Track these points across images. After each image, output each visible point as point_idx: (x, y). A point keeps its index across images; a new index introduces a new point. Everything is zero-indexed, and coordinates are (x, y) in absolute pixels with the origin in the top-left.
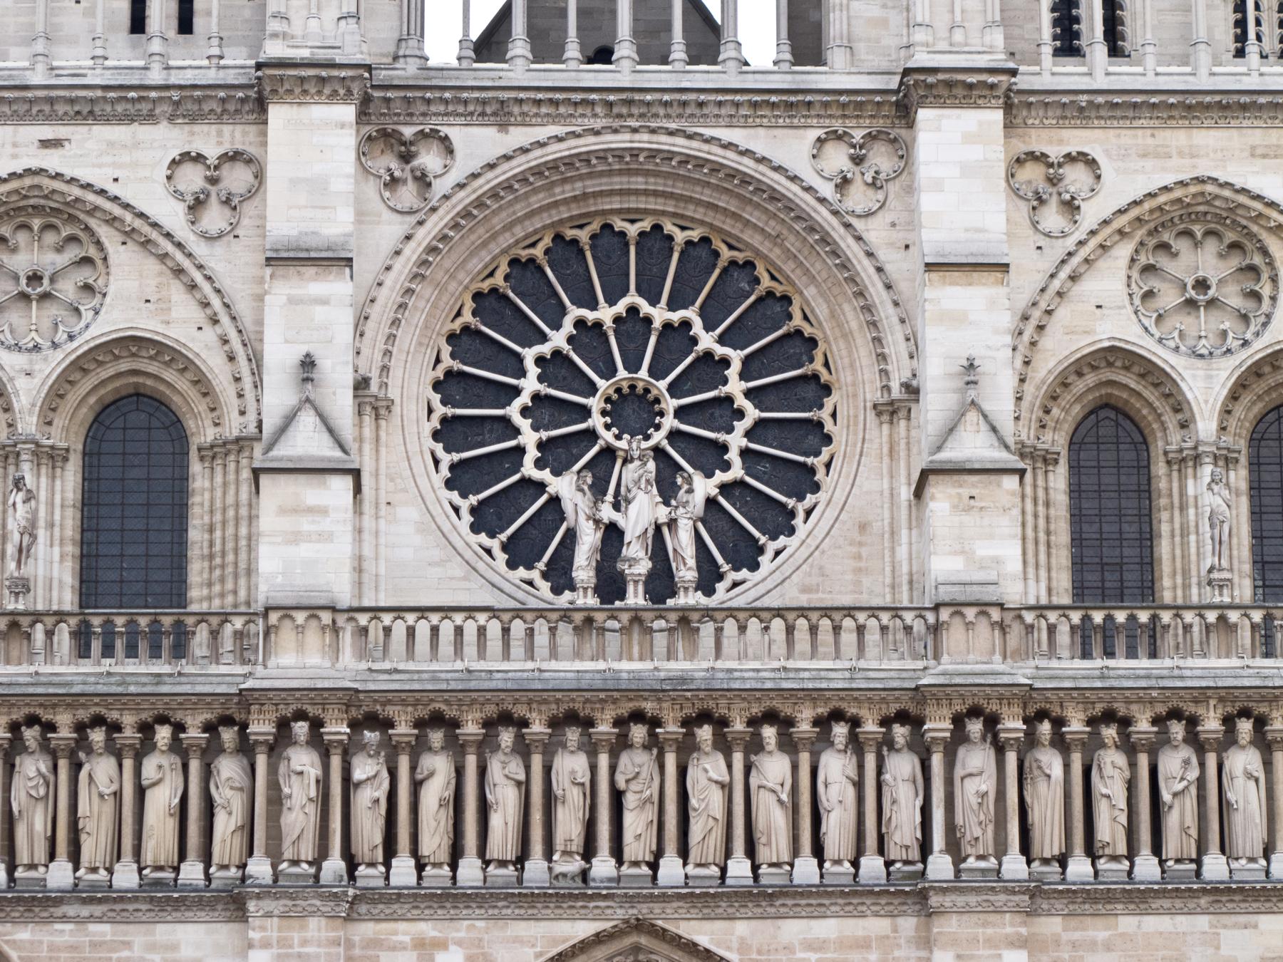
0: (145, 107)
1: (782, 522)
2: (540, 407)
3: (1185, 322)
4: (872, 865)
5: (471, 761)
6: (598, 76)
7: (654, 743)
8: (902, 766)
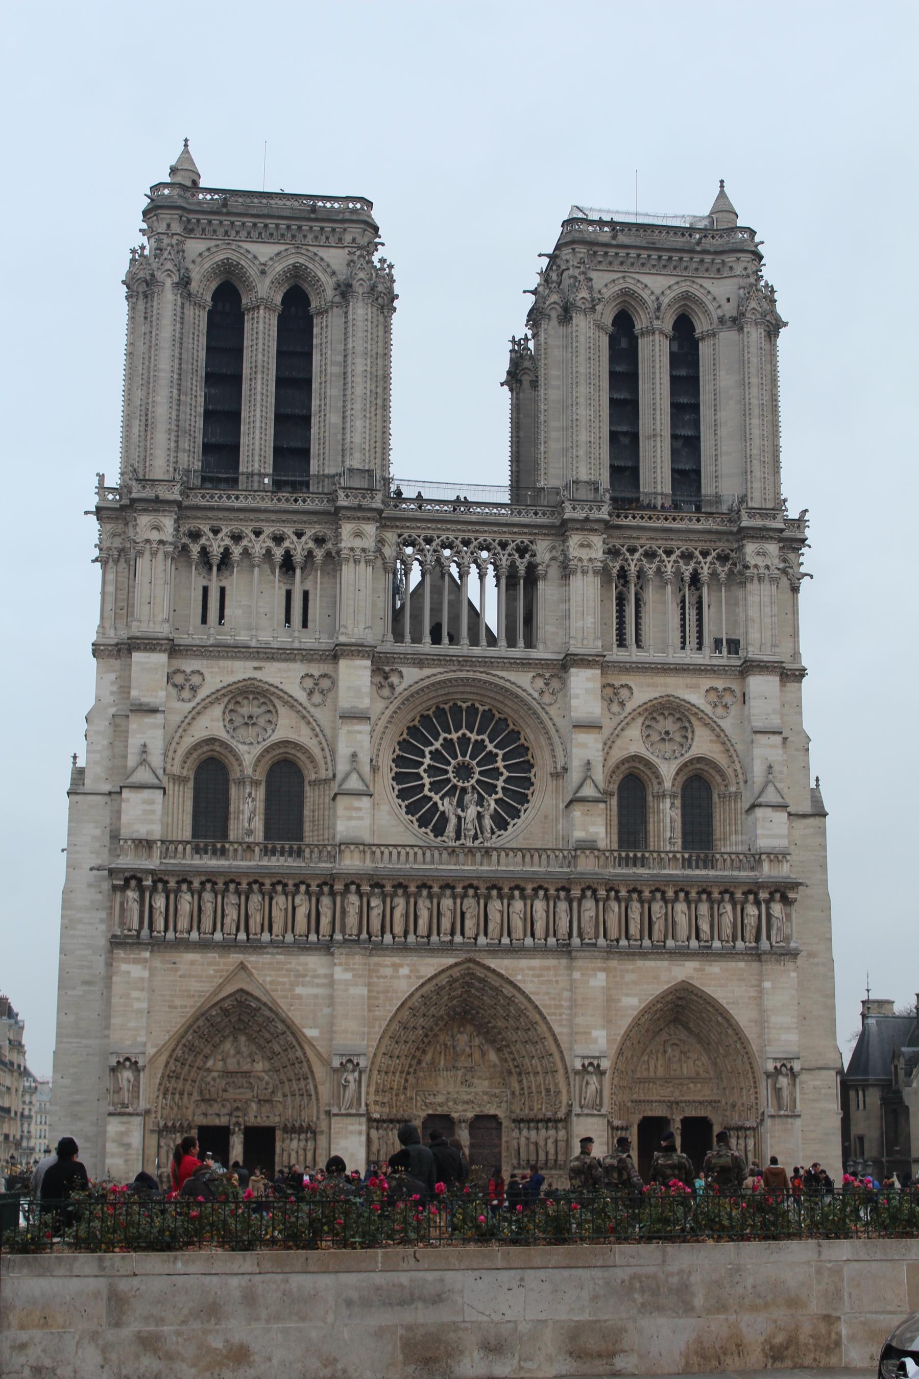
0: (292, 656)
1: (516, 814)
2: (431, 770)
3: (661, 746)
4: (552, 941)
5: (412, 900)
6: (454, 650)
7: (476, 895)
8: (563, 906)
